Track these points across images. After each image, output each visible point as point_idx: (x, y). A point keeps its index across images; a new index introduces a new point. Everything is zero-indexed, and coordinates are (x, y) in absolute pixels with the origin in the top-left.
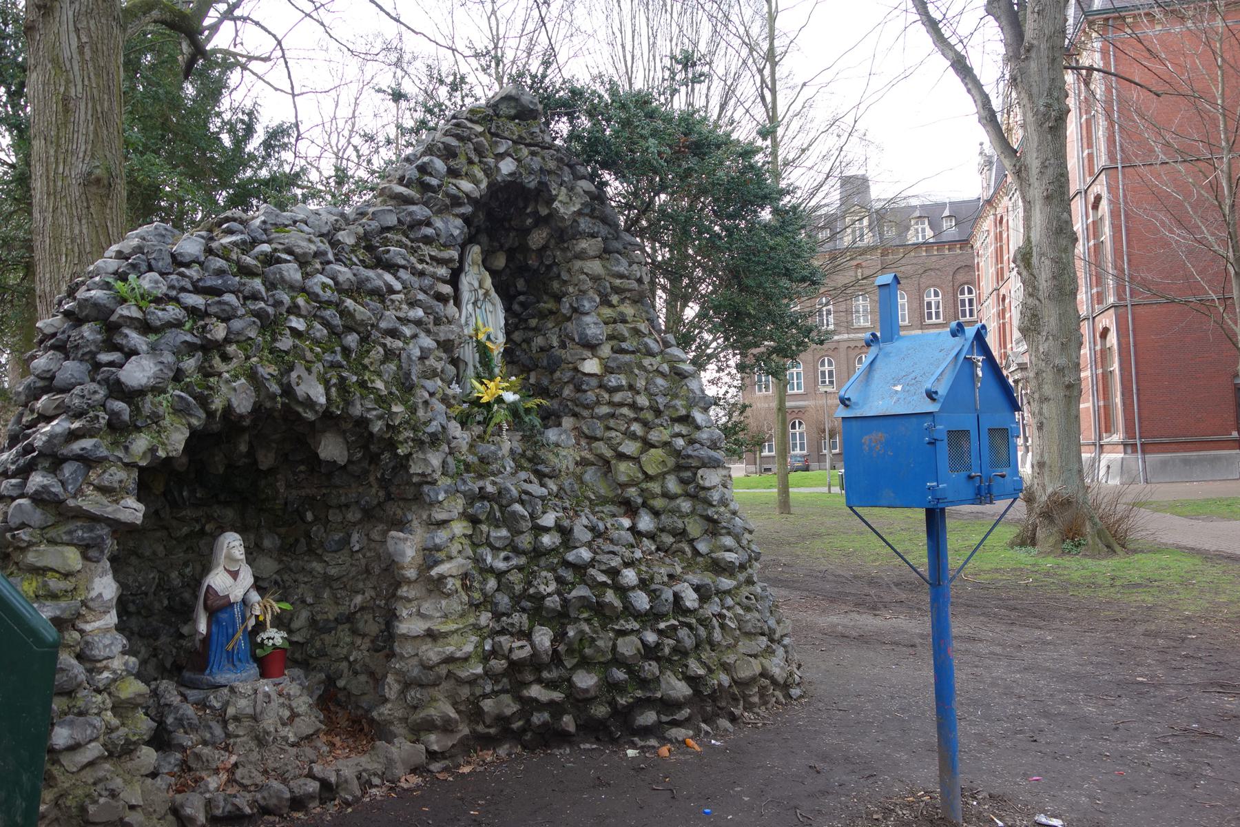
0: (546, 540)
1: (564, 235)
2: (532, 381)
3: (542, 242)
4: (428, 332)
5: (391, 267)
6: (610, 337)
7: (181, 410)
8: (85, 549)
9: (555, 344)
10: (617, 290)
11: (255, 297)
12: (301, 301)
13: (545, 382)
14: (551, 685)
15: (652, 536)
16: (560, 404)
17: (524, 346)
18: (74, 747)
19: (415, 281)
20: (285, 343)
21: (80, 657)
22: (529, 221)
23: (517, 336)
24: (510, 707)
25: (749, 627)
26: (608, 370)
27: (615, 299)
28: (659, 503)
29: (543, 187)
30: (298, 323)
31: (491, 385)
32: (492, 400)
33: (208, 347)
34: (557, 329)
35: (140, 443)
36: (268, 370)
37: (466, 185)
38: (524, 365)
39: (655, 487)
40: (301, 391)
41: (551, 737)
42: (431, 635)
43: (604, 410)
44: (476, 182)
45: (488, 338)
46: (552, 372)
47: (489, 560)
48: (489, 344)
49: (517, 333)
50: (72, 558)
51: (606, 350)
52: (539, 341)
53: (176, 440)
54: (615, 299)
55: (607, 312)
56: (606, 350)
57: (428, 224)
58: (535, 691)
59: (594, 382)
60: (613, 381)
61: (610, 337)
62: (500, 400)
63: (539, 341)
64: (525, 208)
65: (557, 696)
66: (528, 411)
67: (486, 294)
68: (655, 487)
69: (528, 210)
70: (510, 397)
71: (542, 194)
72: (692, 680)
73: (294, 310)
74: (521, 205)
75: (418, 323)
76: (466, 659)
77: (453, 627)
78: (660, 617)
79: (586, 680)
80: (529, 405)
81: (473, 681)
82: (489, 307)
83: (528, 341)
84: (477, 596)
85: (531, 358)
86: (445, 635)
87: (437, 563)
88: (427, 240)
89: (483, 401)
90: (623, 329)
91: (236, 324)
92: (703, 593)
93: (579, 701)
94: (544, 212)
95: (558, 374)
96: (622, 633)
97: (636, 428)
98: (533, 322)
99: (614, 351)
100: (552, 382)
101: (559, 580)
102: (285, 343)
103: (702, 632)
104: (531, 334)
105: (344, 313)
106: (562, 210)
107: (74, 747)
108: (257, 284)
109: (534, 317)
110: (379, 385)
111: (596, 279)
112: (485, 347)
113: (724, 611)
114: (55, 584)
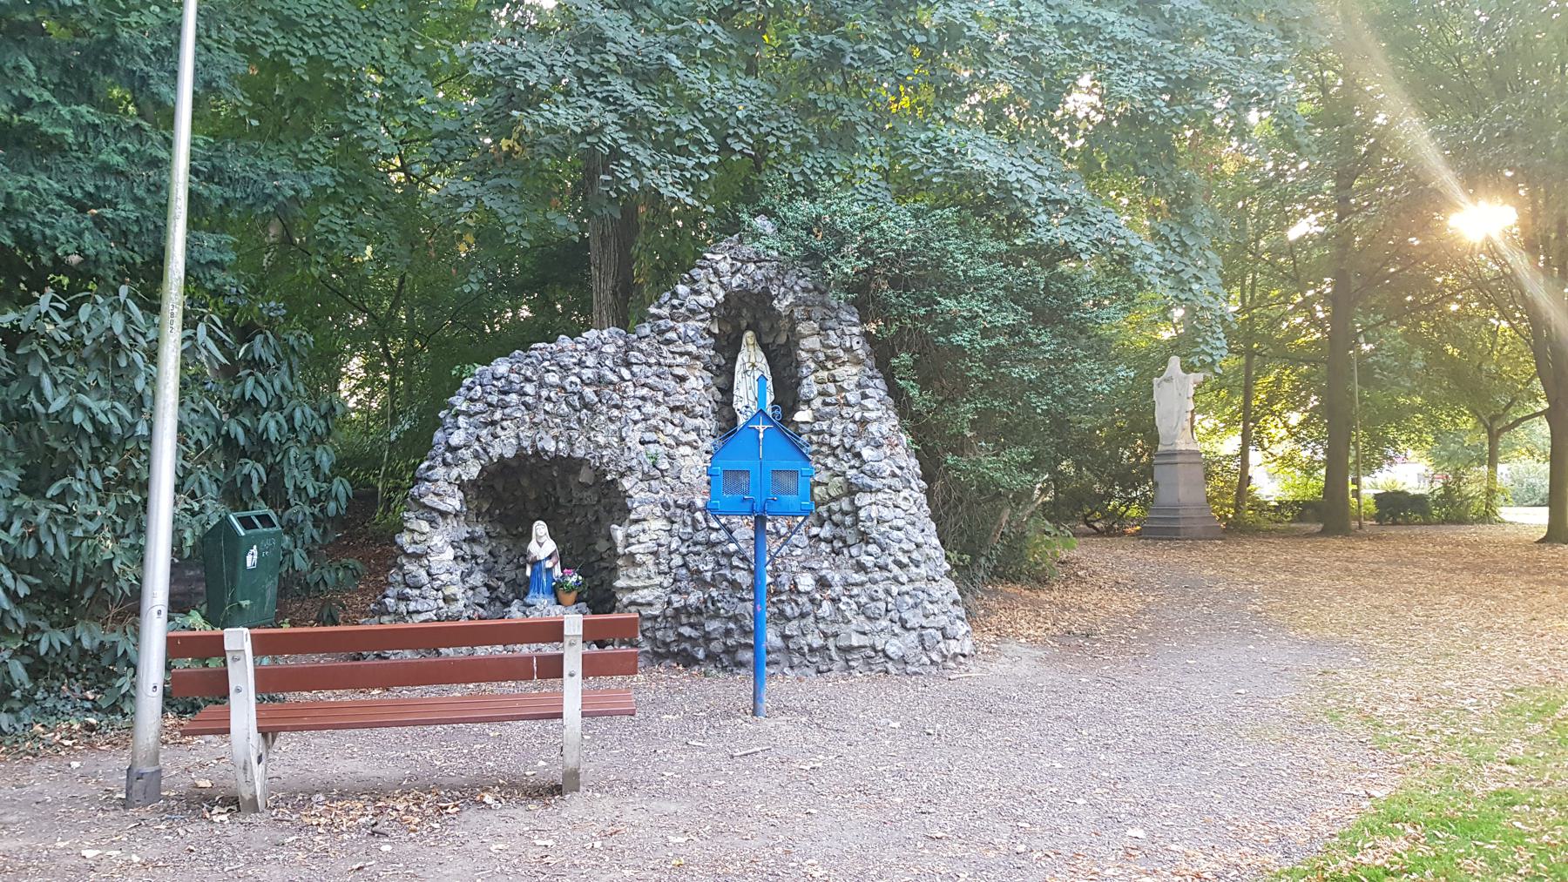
0: (713, 536)
1: (794, 323)
4: (657, 404)
5: (628, 365)
6: (820, 394)
7: (477, 456)
8: (431, 522)
10: (828, 358)
11: (525, 394)
12: (552, 394)
14: (692, 626)
15: (829, 541)
18: (418, 612)
19: (649, 371)
20: (540, 417)
21: (429, 574)
24: (671, 637)
25: (869, 613)
26: (816, 419)
27: (829, 364)
28: (837, 518)
29: (766, 290)
30: (549, 406)
33: (493, 423)
35: (455, 472)
36: (526, 433)
37: (705, 299)
39: (835, 506)
40: (539, 445)
41: (689, 661)
42: (632, 589)
43: (815, 447)
44: (714, 296)
47: (674, 546)
50: (425, 526)
51: (817, 403)
53: (474, 470)
54: (829, 364)
55: (824, 374)
56: (817, 403)
57: (672, 329)
58: (686, 631)
59: (806, 428)
60: (817, 427)
61: (820, 394)
65: (694, 634)
68: (835, 506)
71: (766, 297)
72: (785, 638)
73: (548, 399)
75: (643, 398)
76: (650, 604)
77: (640, 584)
78: (777, 593)
79: (712, 626)
81: (655, 618)
84: (664, 568)
86: (637, 588)
87: (630, 545)
88: (669, 342)
90: (832, 388)
91: (507, 411)
92: (823, 583)
93: (707, 638)
96: (742, 600)
97: (830, 461)
99: (825, 404)
101: (718, 563)
102: (540, 417)
103: (808, 607)
105: (581, 398)
107: (418, 612)
108: (529, 388)
110: (601, 440)
111: (813, 351)
113: (844, 599)
114: (417, 537)
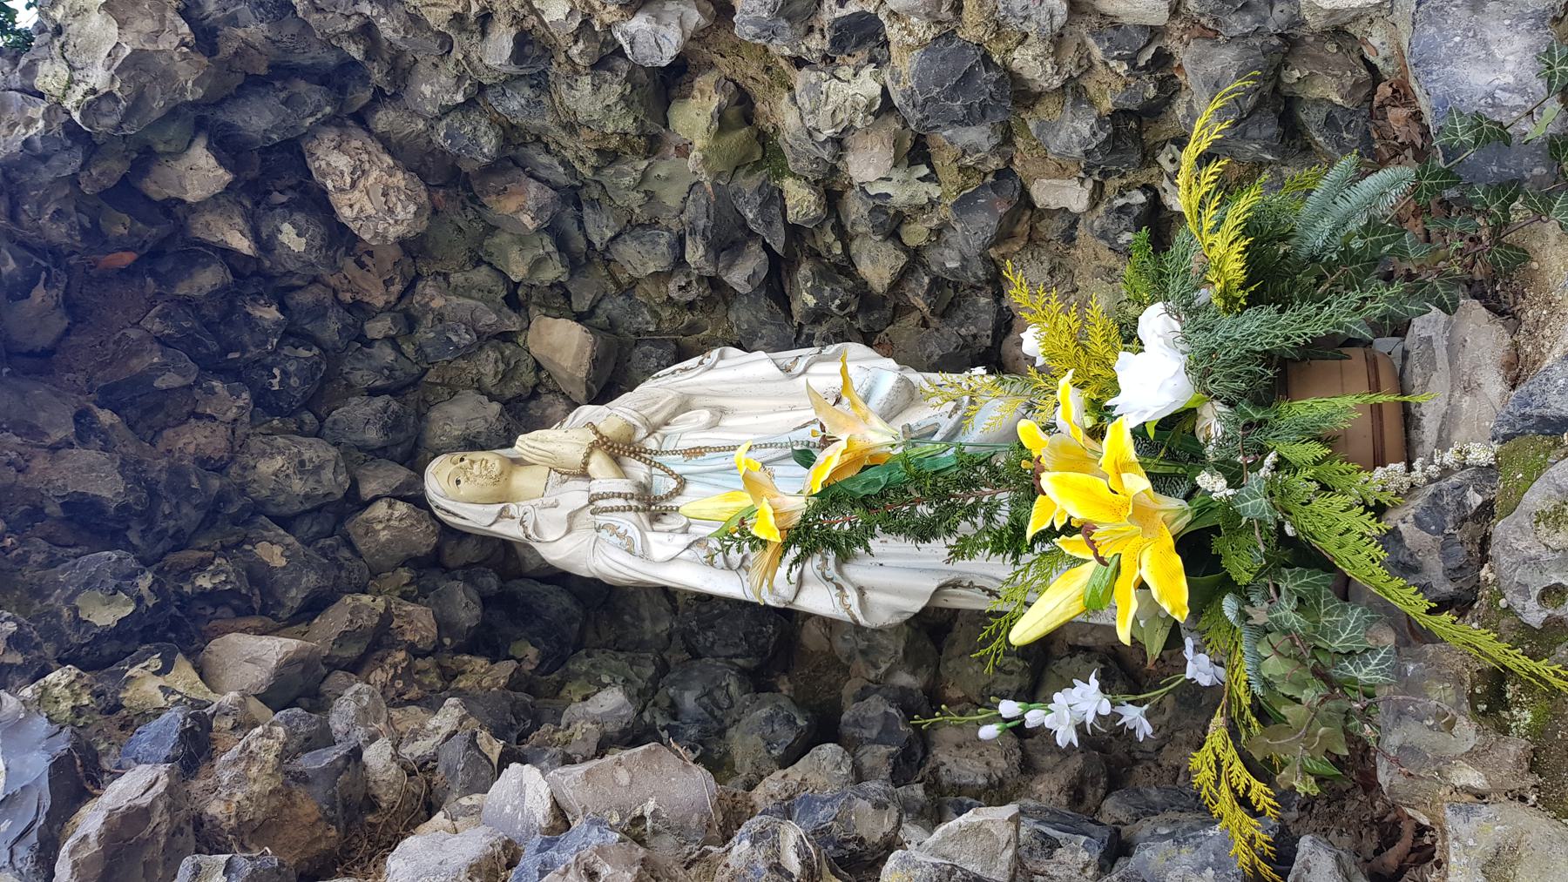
2: (1073, 196)
3: (381, 171)
9: (867, 86)
13: (1075, 130)
16: (1210, 35)
17: (915, 234)
22: (291, 238)
23: (877, 266)
31: (1061, 498)
32: (1174, 511)
34: (801, 78)
38: (1003, 235)
45: (805, 458)
46: (1022, 94)
48: (829, 461)
49: (866, 269)
52: (869, 166)
62: (1170, 446)
63: (869, 166)
64: (227, 254)
66: (1271, 273)
67: (619, 449)
69: (242, 243)
70: (1154, 379)
74: (208, 279)
80: (1218, 249)
82: (689, 431)
83: (891, 224)
85: (964, 205)
89: (1174, 596)
94: (199, 173)
95: (1029, 62)
98: (800, 200)
100: (1074, 91)
104: (856, 209)
106: (98, 77)
109: (773, 199)
112: (831, 497)
